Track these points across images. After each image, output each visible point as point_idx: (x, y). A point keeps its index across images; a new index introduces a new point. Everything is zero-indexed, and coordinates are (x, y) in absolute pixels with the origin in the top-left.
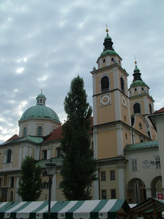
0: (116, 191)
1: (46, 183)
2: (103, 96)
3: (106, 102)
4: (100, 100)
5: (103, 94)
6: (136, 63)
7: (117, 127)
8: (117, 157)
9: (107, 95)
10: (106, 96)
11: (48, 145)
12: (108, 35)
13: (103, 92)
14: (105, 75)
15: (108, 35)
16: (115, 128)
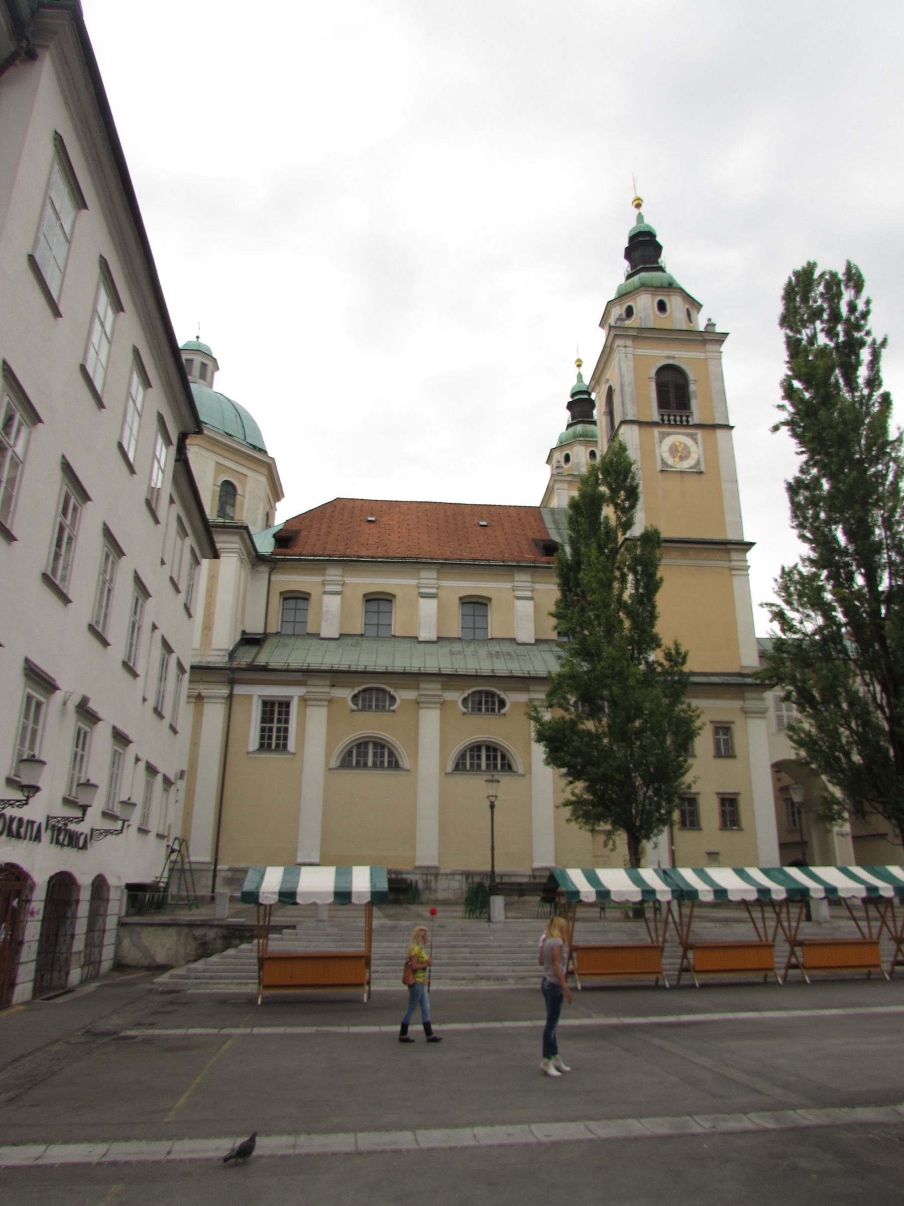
0: (742, 803)
1: (366, 744)
2: (669, 434)
3: (682, 458)
4: (657, 445)
5: (670, 425)
6: (579, 366)
7: (734, 563)
8: (740, 675)
9: (687, 435)
10: (678, 438)
11: (322, 571)
12: (640, 218)
13: (663, 420)
14: (673, 358)
15: (640, 218)
16: (726, 564)
